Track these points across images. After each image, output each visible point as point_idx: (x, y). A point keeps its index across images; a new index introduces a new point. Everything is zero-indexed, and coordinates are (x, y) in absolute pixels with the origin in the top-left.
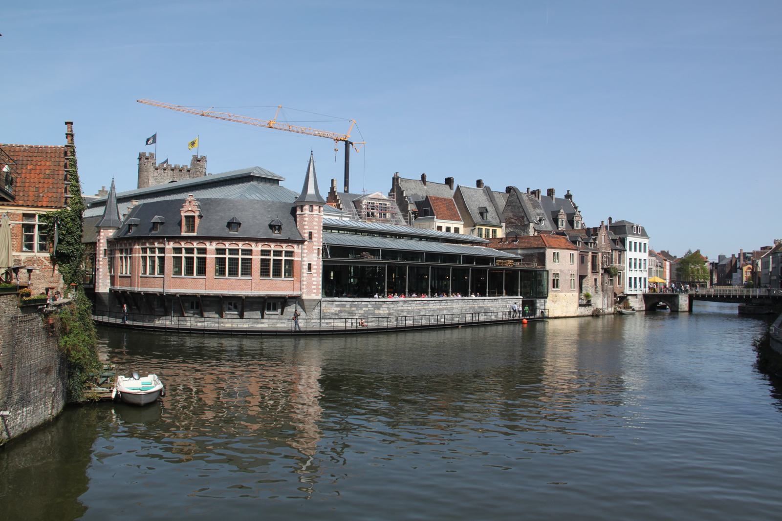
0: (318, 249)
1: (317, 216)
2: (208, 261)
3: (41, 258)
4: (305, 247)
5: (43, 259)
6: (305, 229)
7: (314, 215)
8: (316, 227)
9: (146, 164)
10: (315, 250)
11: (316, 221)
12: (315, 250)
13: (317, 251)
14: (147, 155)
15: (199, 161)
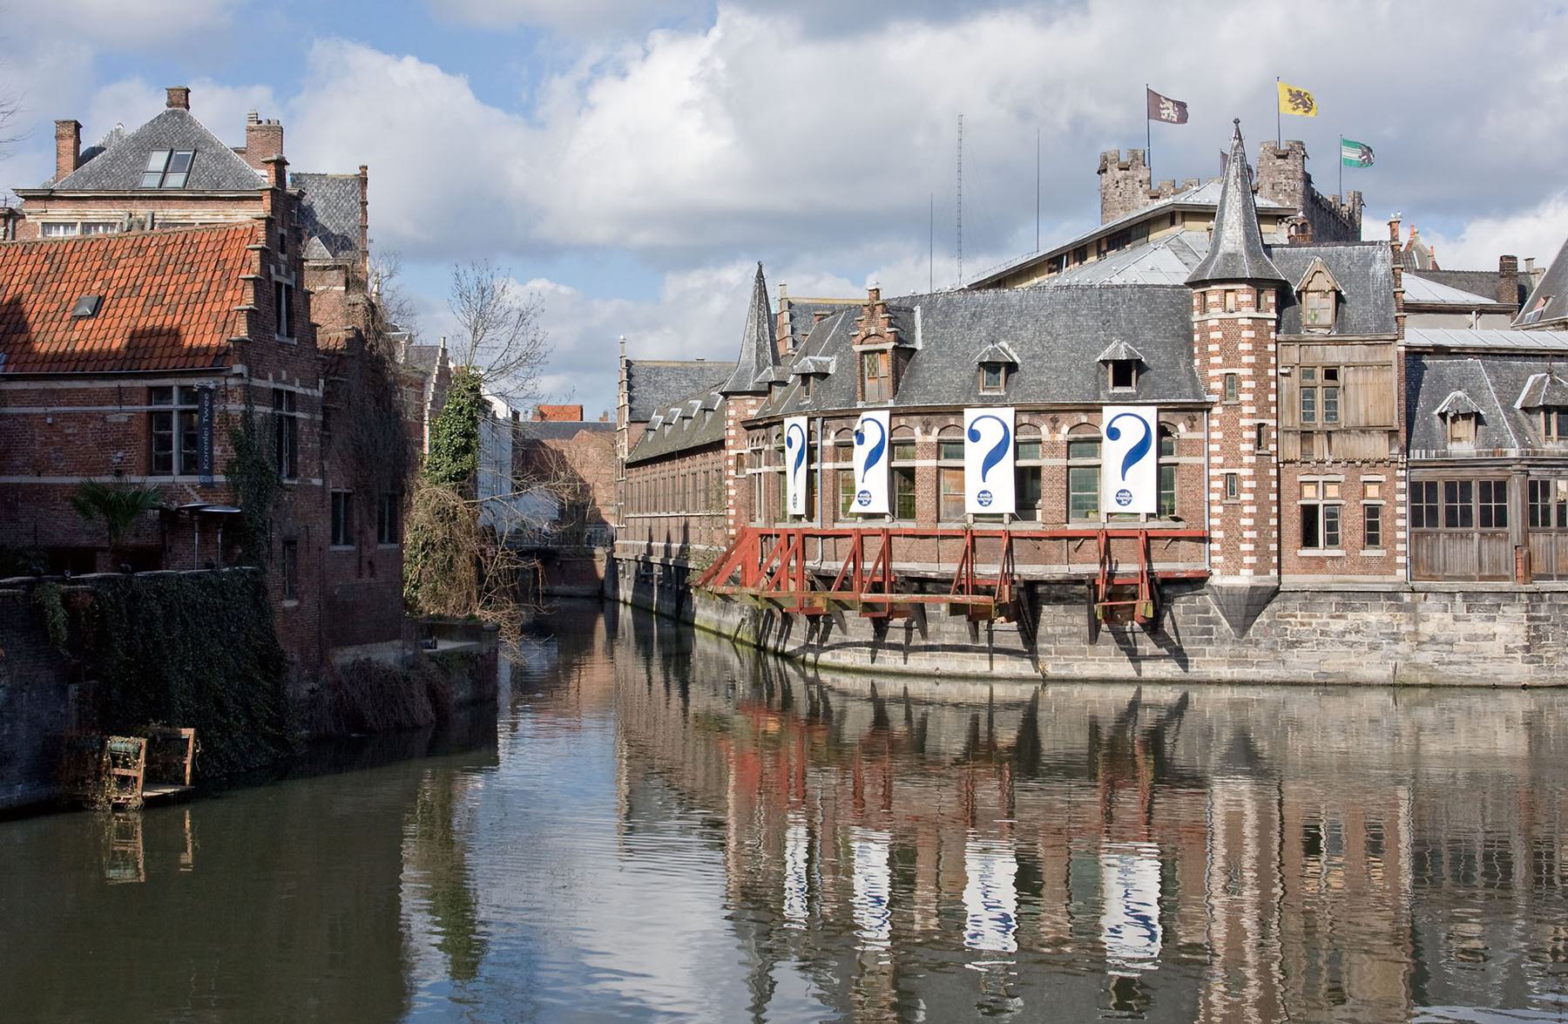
0: (1260, 425)
1: (1250, 322)
2: (917, 471)
3: (186, 487)
4: (1215, 423)
5: (189, 490)
6: (1214, 366)
7: (1241, 322)
8: (1245, 359)
9: (1121, 185)
10: (1251, 428)
11: (1214, 341)
12: (1251, 428)
13: (1253, 435)
14: (1124, 159)
15: (1284, 157)
